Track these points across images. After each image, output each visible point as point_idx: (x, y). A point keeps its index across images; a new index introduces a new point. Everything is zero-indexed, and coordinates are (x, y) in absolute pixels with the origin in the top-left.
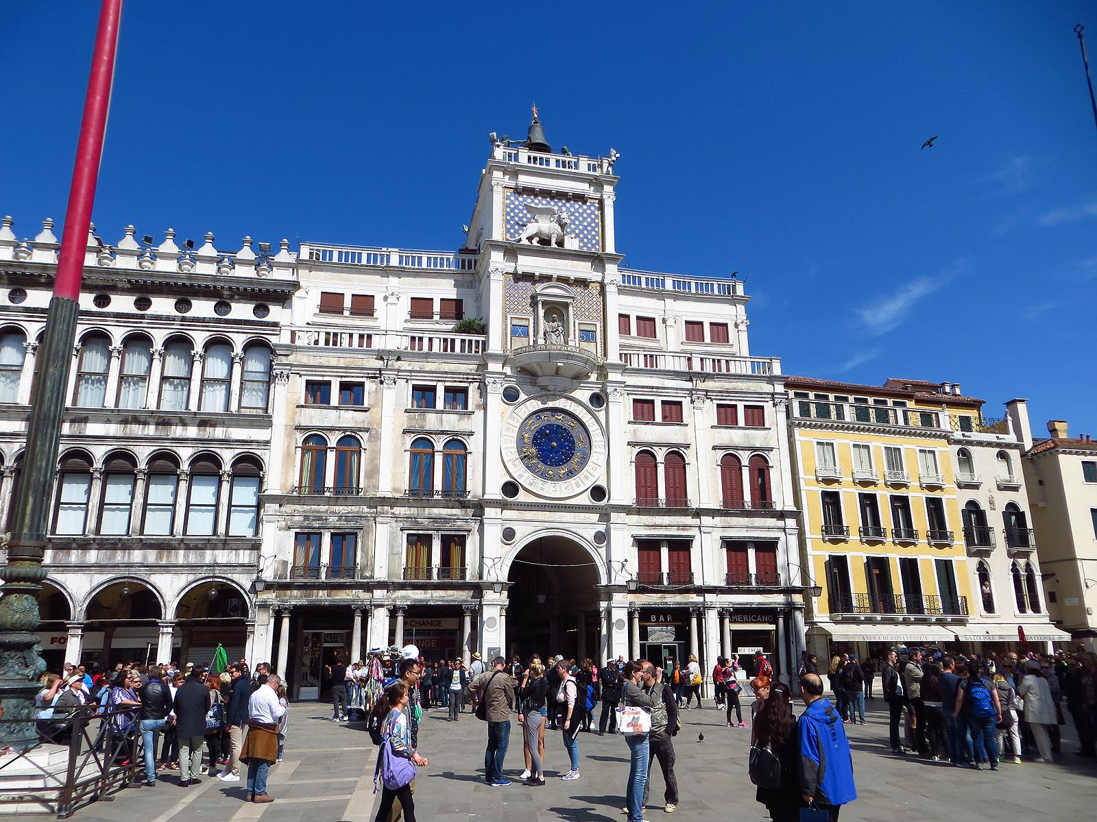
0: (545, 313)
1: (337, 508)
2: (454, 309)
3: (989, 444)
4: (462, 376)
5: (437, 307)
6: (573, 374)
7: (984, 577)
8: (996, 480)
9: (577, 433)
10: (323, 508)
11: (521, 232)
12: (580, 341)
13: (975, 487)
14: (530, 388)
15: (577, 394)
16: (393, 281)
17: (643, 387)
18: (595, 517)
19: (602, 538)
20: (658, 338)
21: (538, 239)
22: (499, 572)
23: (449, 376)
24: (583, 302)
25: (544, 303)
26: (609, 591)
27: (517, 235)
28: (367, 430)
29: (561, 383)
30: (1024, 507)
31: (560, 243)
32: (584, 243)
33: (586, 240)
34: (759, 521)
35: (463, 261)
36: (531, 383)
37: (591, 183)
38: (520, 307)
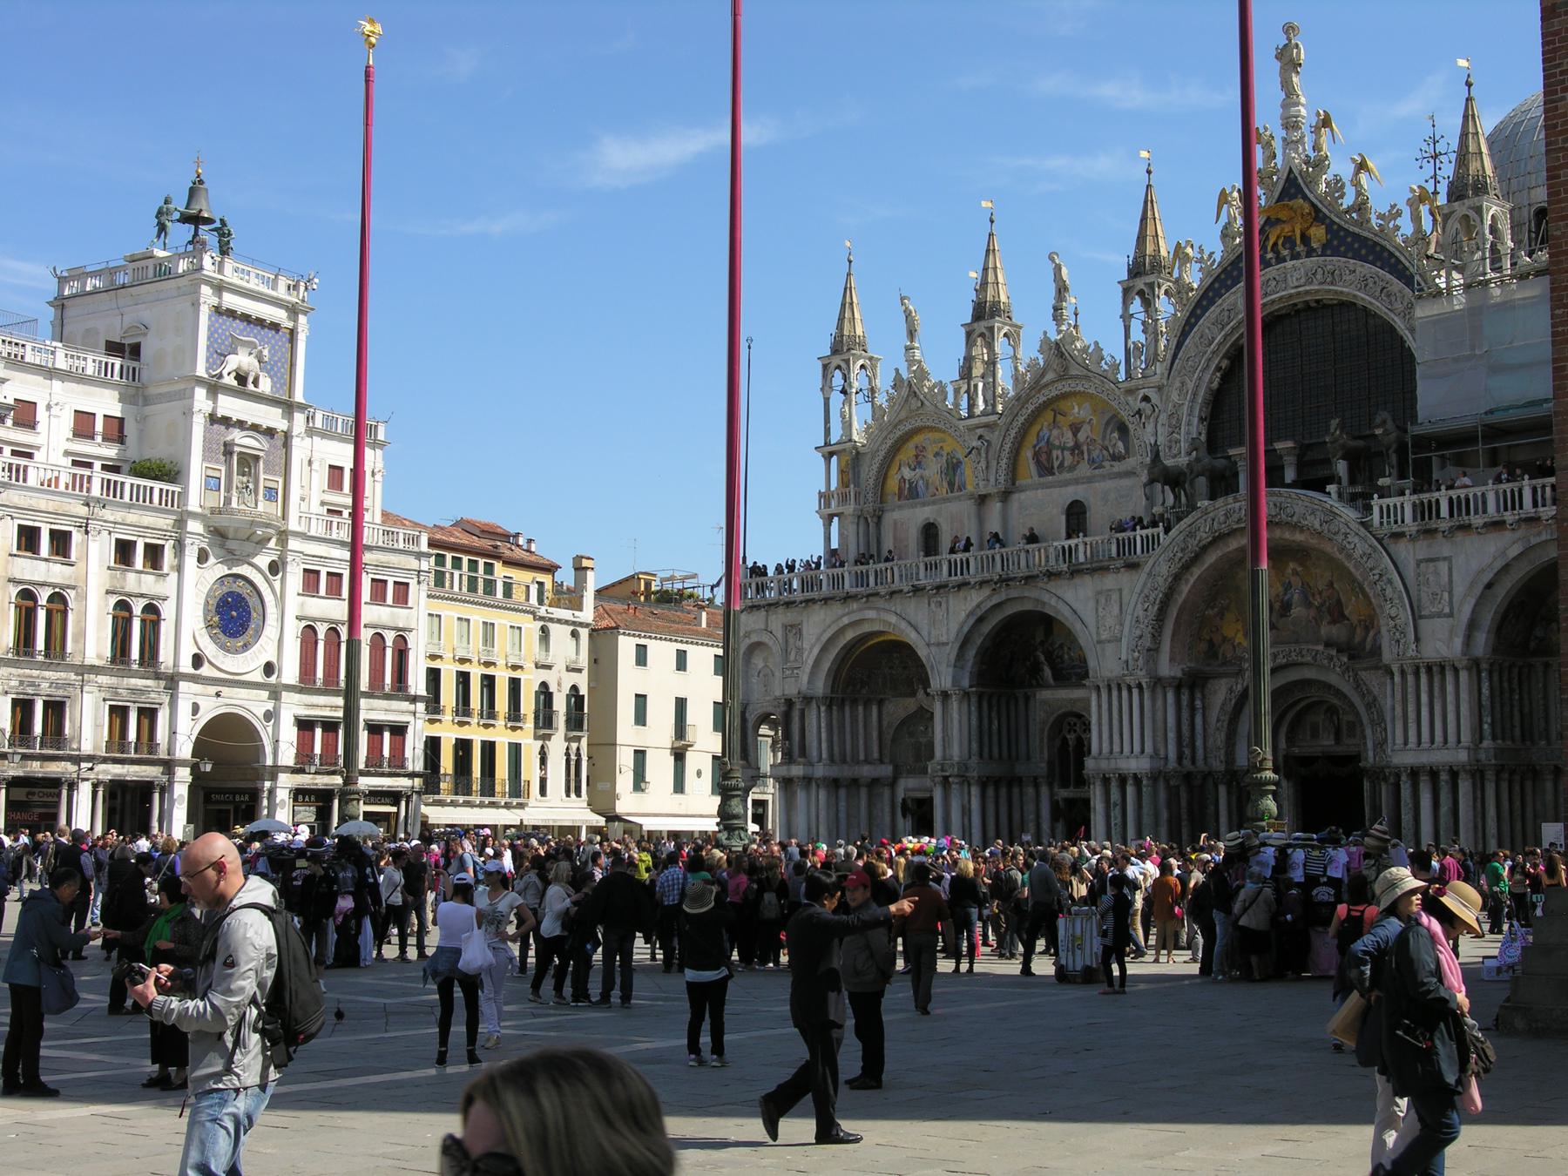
1: (47, 674)
2: (116, 430)
3: (567, 622)
5: (99, 427)
7: (543, 761)
8: (563, 662)
9: (253, 601)
10: (35, 673)
13: (549, 667)
14: (217, 550)
15: (256, 560)
16: (57, 384)
18: (265, 694)
19: (268, 716)
22: (184, 750)
25: (240, 453)
26: (274, 771)
28: (73, 588)
29: (249, 547)
30: (584, 691)
34: (395, 704)
37: (287, 309)
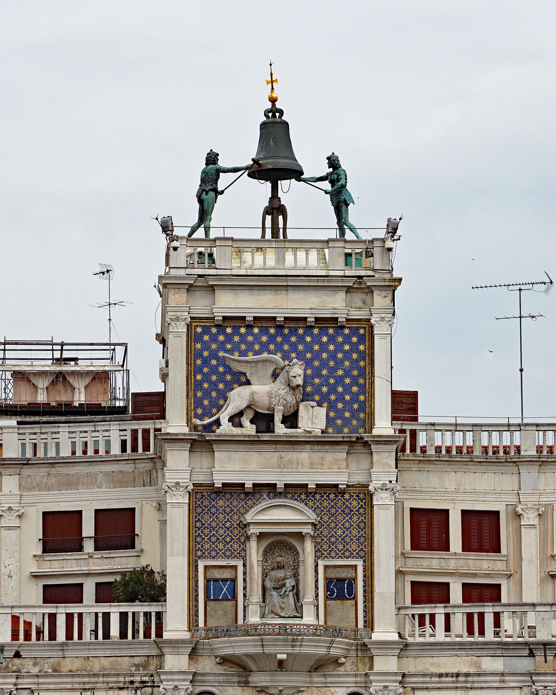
0: (266, 553)
2: (117, 529)
4: (122, 679)
5: (88, 528)
6: (311, 663)
11: (221, 402)
12: (327, 598)
17: (441, 675)
20: (504, 550)
21: (250, 414)
23: (101, 679)
24: (333, 525)
25: (261, 536)
27: (214, 410)
31: (291, 420)
32: (337, 411)
33: (340, 406)
35: (135, 432)
36: (239, 682)
38: (221, 546)
